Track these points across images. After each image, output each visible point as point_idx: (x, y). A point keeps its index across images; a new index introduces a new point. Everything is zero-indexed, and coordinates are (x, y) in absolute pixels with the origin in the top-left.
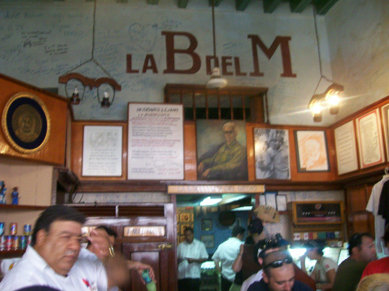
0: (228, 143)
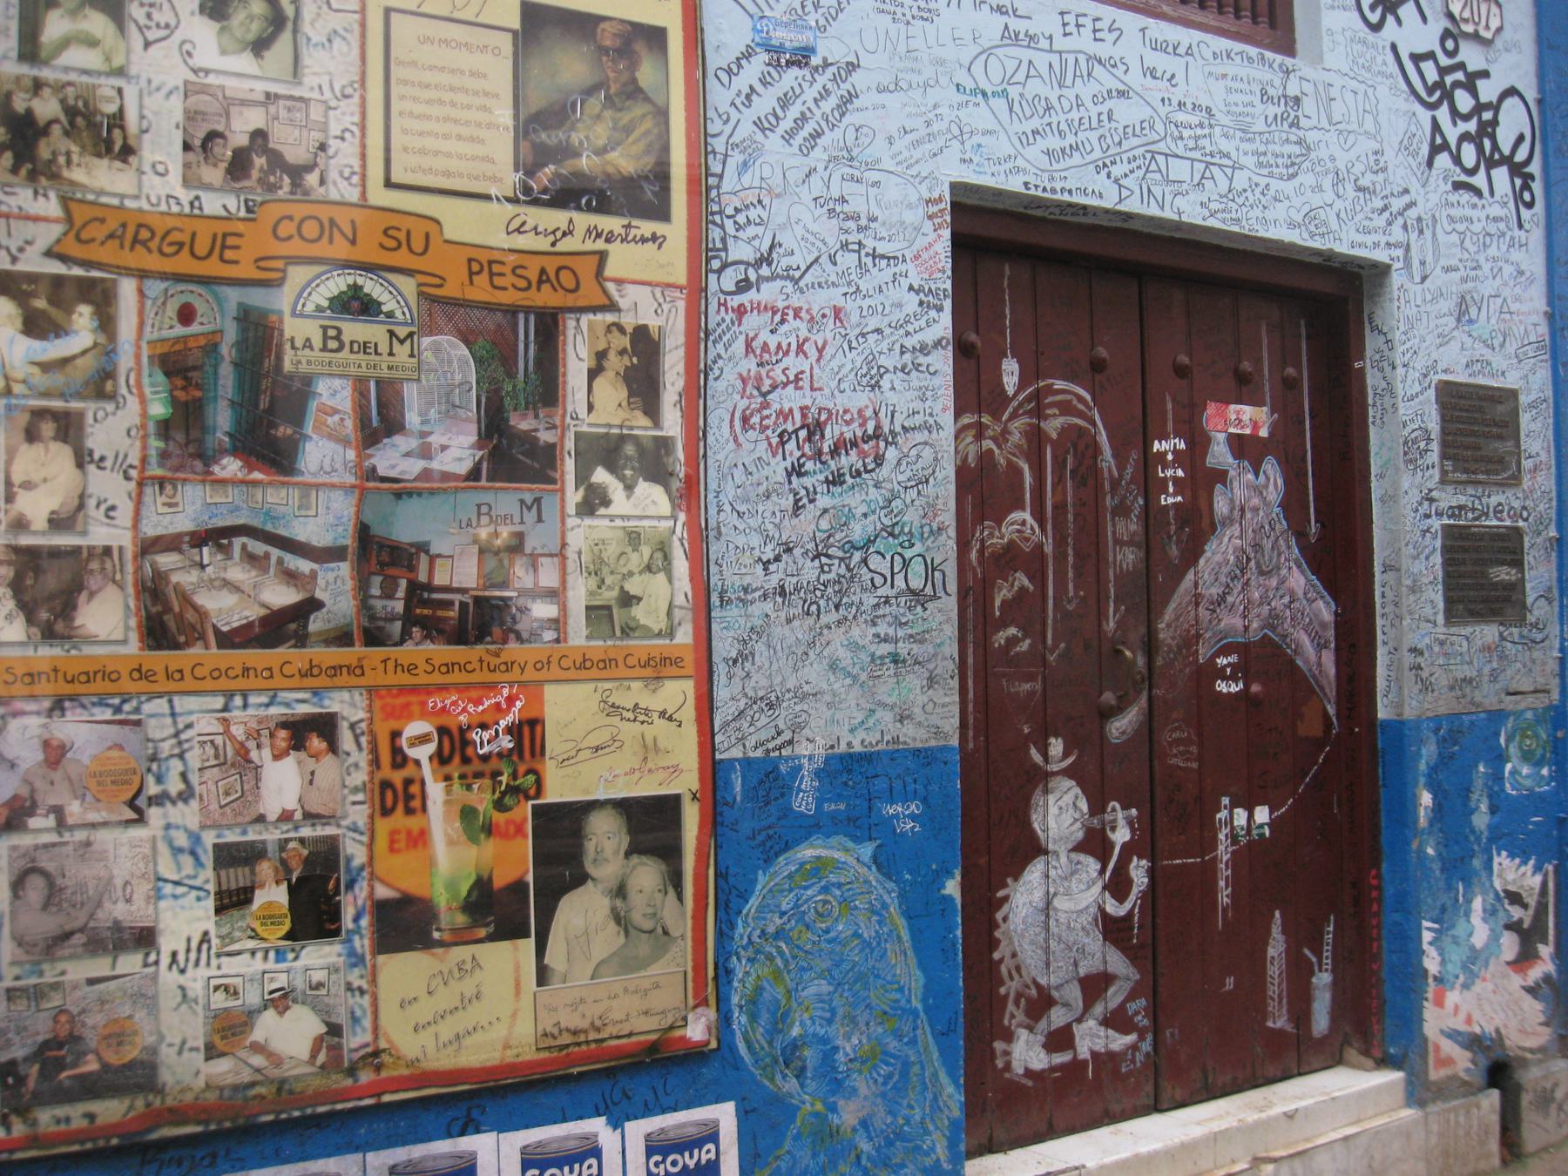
0: (612, 91)
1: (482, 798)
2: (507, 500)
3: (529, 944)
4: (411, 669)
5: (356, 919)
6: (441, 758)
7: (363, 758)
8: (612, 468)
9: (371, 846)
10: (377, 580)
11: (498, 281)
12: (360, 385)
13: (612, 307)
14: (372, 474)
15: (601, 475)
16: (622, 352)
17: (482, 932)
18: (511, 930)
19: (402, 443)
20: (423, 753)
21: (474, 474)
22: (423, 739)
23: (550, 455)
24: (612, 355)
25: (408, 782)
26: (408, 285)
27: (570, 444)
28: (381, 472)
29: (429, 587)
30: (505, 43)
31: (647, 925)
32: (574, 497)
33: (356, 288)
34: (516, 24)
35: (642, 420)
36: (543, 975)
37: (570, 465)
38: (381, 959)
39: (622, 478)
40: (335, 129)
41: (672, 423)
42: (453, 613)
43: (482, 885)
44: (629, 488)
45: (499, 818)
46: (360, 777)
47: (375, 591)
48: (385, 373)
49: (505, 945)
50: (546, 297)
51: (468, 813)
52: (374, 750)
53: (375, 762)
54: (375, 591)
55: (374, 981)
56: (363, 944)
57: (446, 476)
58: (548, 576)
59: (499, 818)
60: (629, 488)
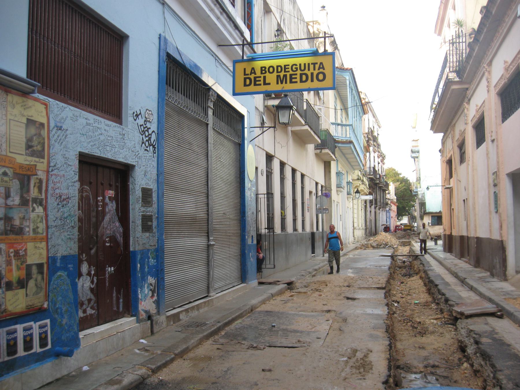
1: (19, 263)
2: (23, 209)
3: (25, 289)
4: (11, 240)
5: (3, 284)
6: (14, 256)
7: (4, 256)
8: (36, 204)
9: (5, 271)
10: (7, 224)
11: (23, 170)
12: (6, 188)
13: (36, 175)
14: (6, 204)
15: (35, 205)
16: (38, 183)
17: (19, 287)
18: (22, 287)
19: (11, 199)
20: (12, 255)
21: (19, 205)
22: (12, 252)
23: (28, 201)
24: (37, 183)
25: (10, 260)
26: (12, 170)
27: (31, 199)
28: (8, 204)
29: (14, 225)
30: (24, 126)
31: (40, 286)
32: (31, 209)
33: (5, 171)
34: (26, 123)
35: (40, 195)
36: (27, 295)
37: (31, 203)
38: (7, 292)
39: (37, 206)
40: (3, 141)
41: (43, 196)
42: (16, 230)
43: (19, 278)
44: (38, 207)
45: (21, 266)
46: (4, 259)
47: (7, 226)
48: (9, 186)
49: (22, 290)
50: (29, 173)
51: (17, 266)
52: (6, 255)
53: (6, 257)
54: (7, 226)
55: (5, 296)
56: (4, 289)
57: (16, 205)
58: (28, 224)
59: (21, 266)
60: (38, 207)
